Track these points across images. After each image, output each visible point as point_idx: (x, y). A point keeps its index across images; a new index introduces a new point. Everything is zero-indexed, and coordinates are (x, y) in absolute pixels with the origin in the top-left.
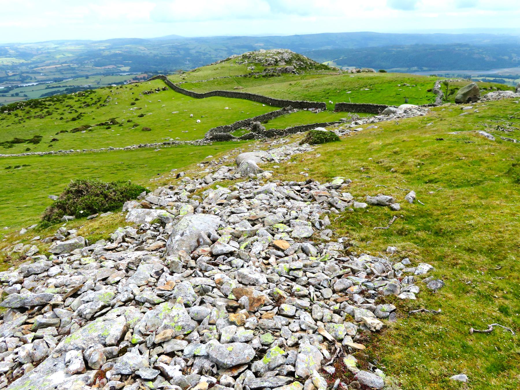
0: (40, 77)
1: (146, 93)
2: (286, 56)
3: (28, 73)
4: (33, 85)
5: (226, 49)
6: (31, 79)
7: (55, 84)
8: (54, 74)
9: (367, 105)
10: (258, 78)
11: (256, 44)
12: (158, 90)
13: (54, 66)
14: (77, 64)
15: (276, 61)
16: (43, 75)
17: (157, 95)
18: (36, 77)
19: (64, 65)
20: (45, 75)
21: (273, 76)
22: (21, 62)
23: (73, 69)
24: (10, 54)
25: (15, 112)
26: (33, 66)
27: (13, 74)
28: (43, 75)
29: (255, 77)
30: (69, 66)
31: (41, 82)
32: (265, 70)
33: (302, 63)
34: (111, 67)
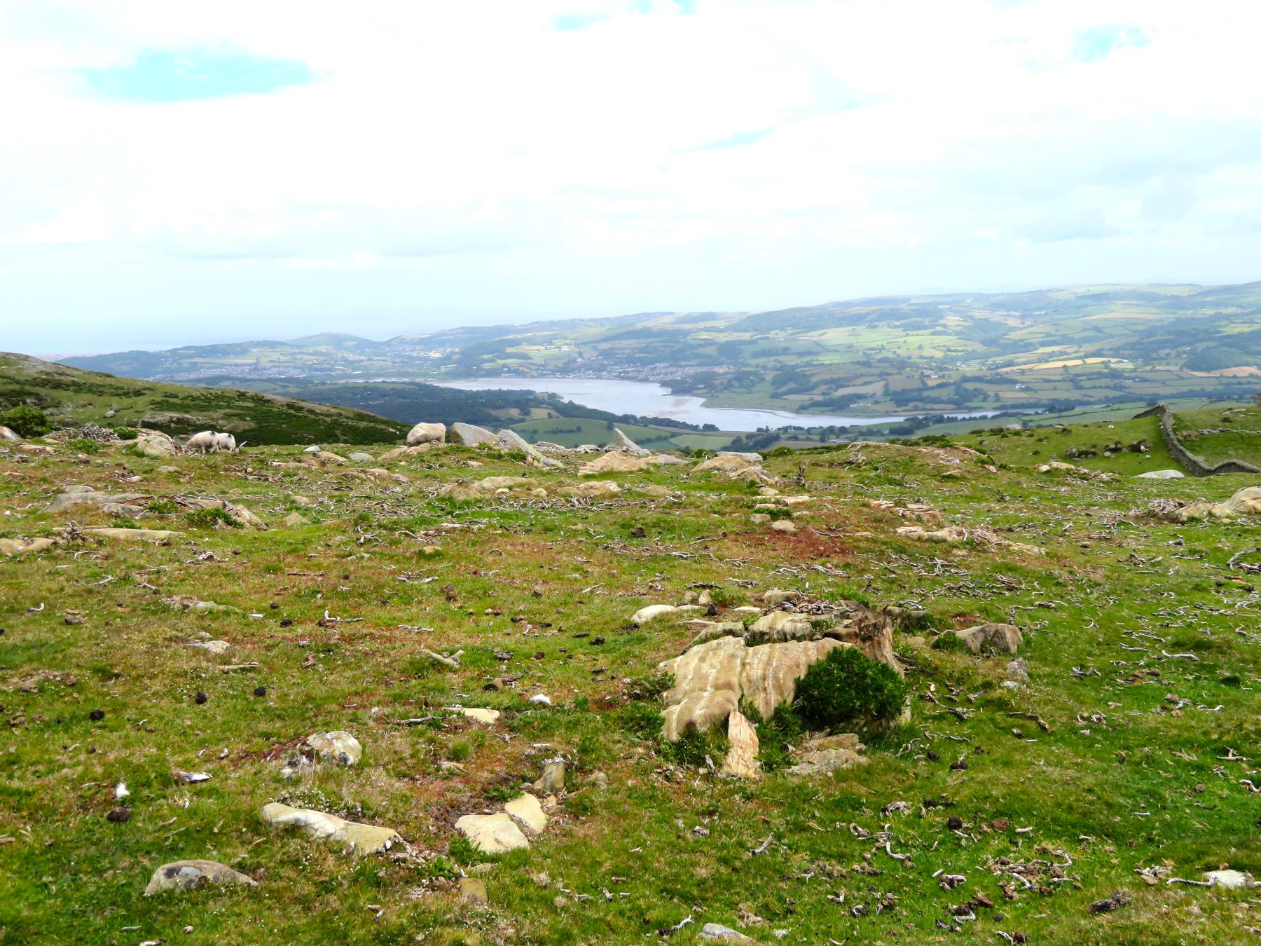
0: (1011, 395)
4: (984, 418)
6: (984, 400)
7: (1047, 418)
8: (1055, 389)
13: (1061, 364)
14: (1132, 358)
16: (1021, 390)
18: (1001, 394)
19: (1089, 361)
20: (1027, 389)
22: (970, 349)
23: (1115, 374)
24: (944, 326)
26: (999, 360)
27: (939, 382)
28: (1021, 390)
30: (1106, 364)
31: (1007, 411)
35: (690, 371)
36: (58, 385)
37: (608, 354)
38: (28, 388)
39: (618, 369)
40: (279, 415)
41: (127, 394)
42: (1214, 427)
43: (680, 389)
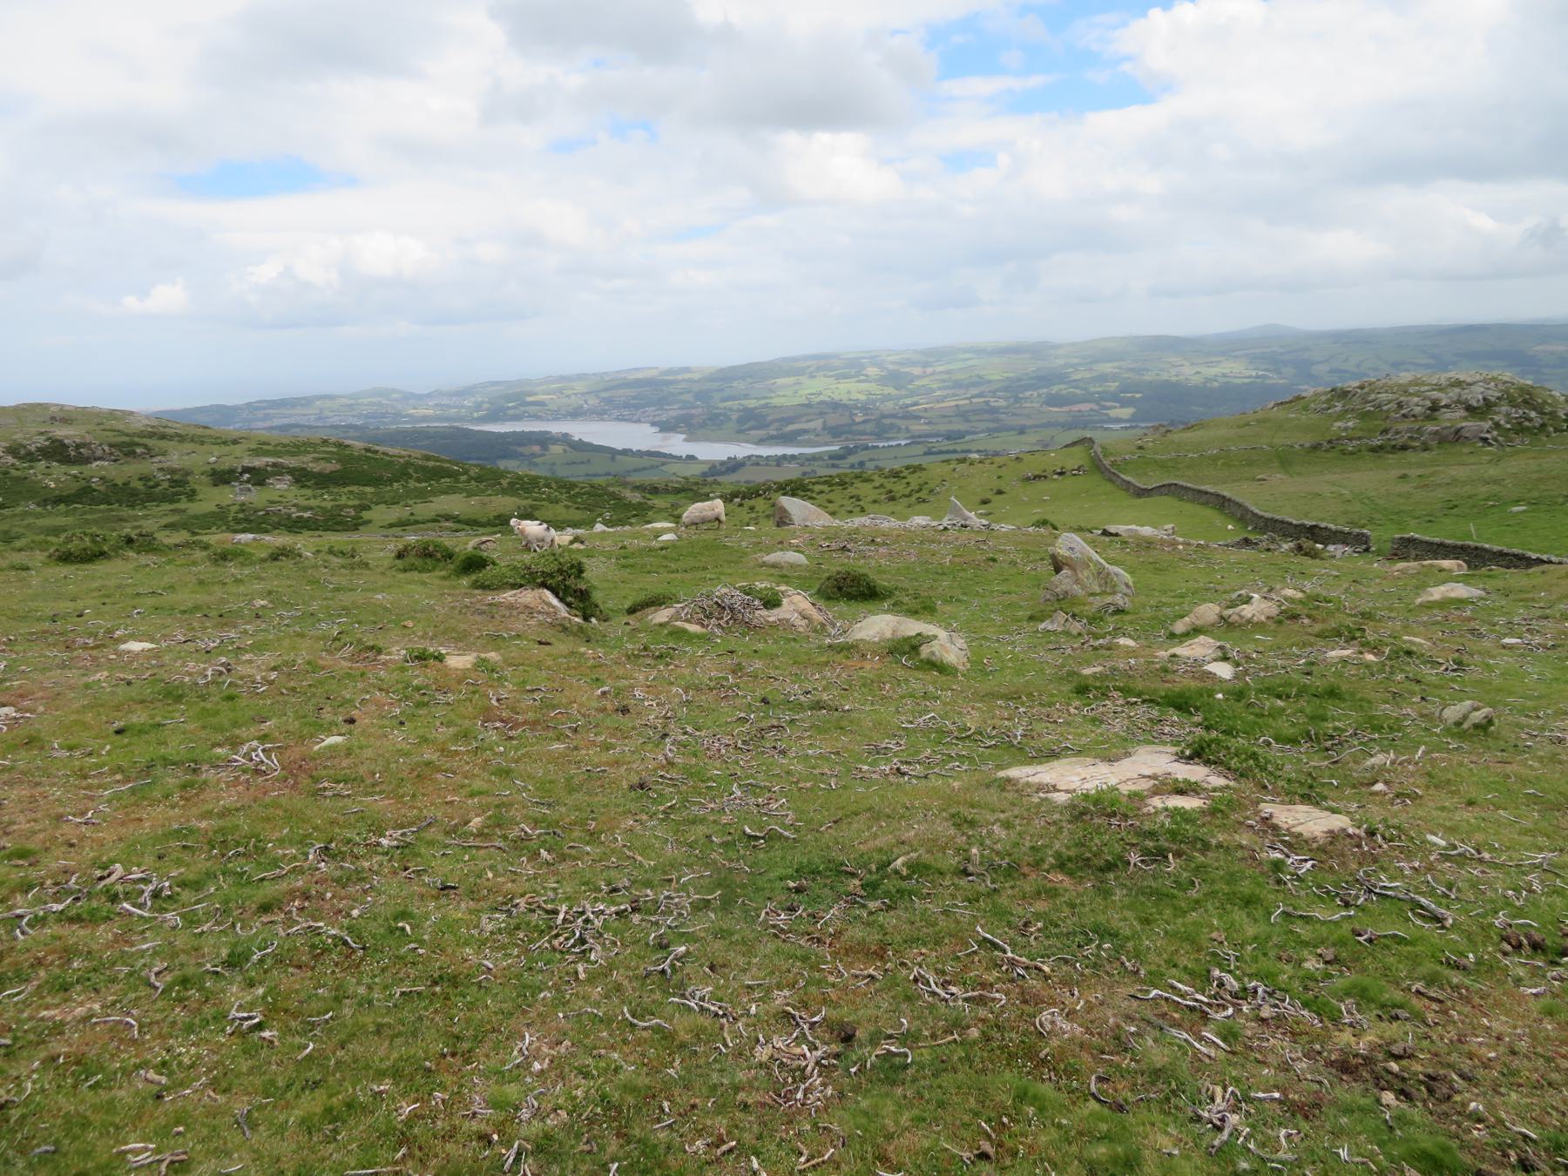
0: (918, 427)
1: (1028, 479)
2: (1475, 396)
3: (894, 416)
5: (1431, 361)
7: (946, 445)
9: (1476, 548)
10: (1352, 453)
11: (1539, 348)
12: (1061, 474)
14: (1006, 399)
15: (1435, 407)
17: (1053, 485)
21: (1404, 448)
23: (994, 410)
25: (752, 502)
26: (908, 401)
29: (1343, 452)
30: (987, 403)
31: (916, 440)
32: (1385, 431)
33: (1533, 414)
34: (1085, 407)
35: (673, 414)
36: (163, 437)
37: (609, 401)
38: (137, 439)
39: (616, 413)
40: (360, 458)
41: (225, 443)
42: (1133, 453)
43: (666, 427)
